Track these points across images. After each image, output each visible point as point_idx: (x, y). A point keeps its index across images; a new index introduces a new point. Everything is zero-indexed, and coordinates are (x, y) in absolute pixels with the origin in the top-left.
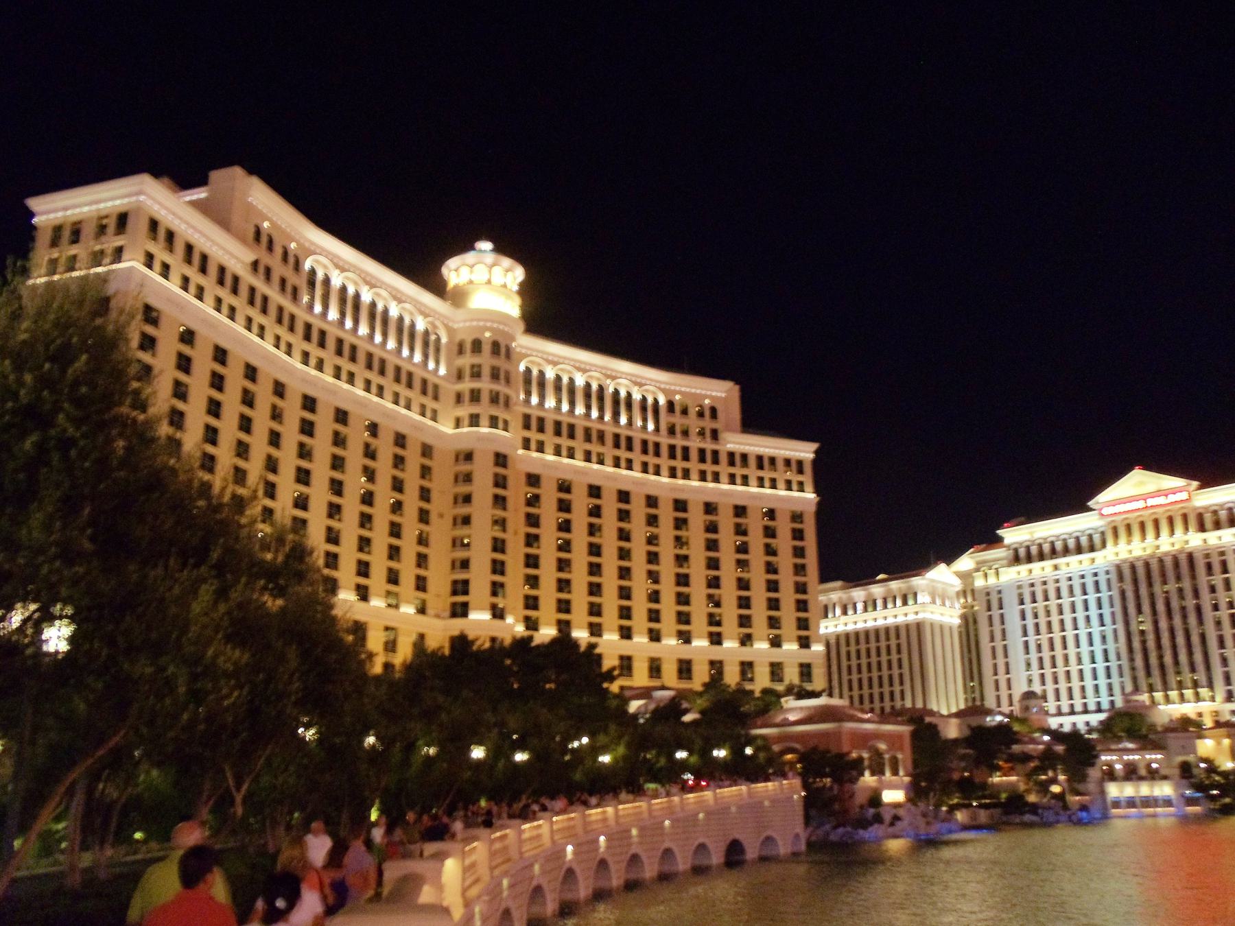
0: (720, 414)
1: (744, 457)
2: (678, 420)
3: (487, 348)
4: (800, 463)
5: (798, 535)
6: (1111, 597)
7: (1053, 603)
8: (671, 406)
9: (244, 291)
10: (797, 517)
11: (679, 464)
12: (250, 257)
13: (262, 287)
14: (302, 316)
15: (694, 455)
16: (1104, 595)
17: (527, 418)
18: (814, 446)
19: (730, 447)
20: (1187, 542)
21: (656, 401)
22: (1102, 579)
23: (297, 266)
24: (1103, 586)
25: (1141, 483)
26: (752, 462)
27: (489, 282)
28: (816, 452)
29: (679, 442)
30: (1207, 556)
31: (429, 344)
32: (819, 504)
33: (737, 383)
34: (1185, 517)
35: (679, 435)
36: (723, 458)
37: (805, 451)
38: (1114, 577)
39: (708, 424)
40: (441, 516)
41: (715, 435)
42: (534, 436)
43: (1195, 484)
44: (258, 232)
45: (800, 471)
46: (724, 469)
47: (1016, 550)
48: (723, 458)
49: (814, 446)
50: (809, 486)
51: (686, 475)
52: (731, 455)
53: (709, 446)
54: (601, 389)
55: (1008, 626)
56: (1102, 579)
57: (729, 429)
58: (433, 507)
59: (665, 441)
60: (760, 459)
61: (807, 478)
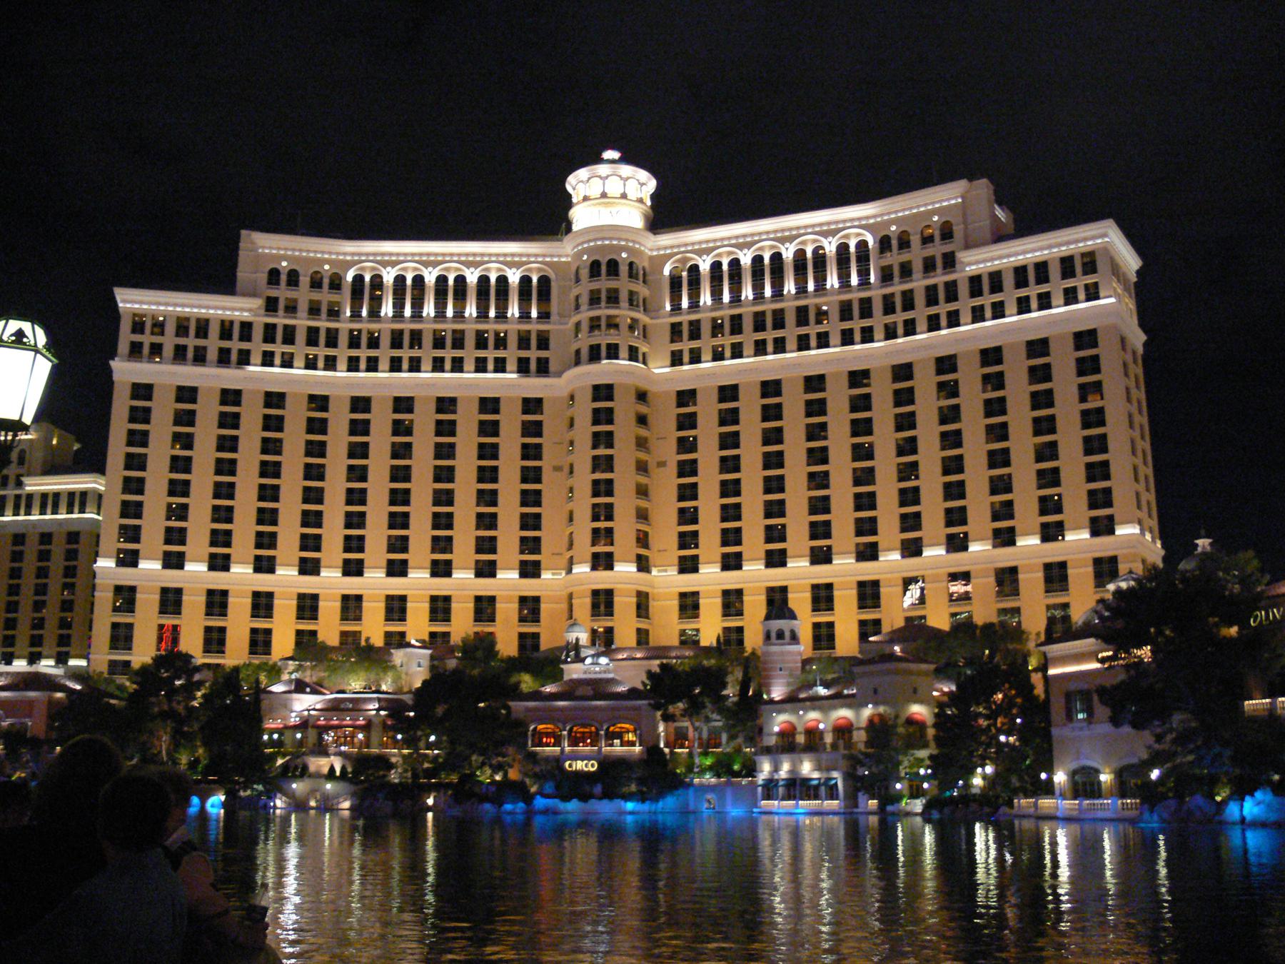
0: (958, 230)
2: (894, 258)
3: (585, 273)
8: (884, 244)
9: (258, 334)
12: (258, 303)
13: (280, 320)
14: (344, 326)
17: (676, 331)
19: (972, 270)
21: (862, 245)
27: (610, 197)
31: (538, 291)
33: (971, 177)
36: (963, 290)
39: (937, 249)
40: (558, 469)
41: (950, 261)
42: (686, 346)
44: (274, 276)
46: (965, 304)
48: (963, 290)
52: (975, 281)
53: (940, 279)
54: (777, 257)
57: (967, 246)
58: (546, 464)
59: (876, 294)
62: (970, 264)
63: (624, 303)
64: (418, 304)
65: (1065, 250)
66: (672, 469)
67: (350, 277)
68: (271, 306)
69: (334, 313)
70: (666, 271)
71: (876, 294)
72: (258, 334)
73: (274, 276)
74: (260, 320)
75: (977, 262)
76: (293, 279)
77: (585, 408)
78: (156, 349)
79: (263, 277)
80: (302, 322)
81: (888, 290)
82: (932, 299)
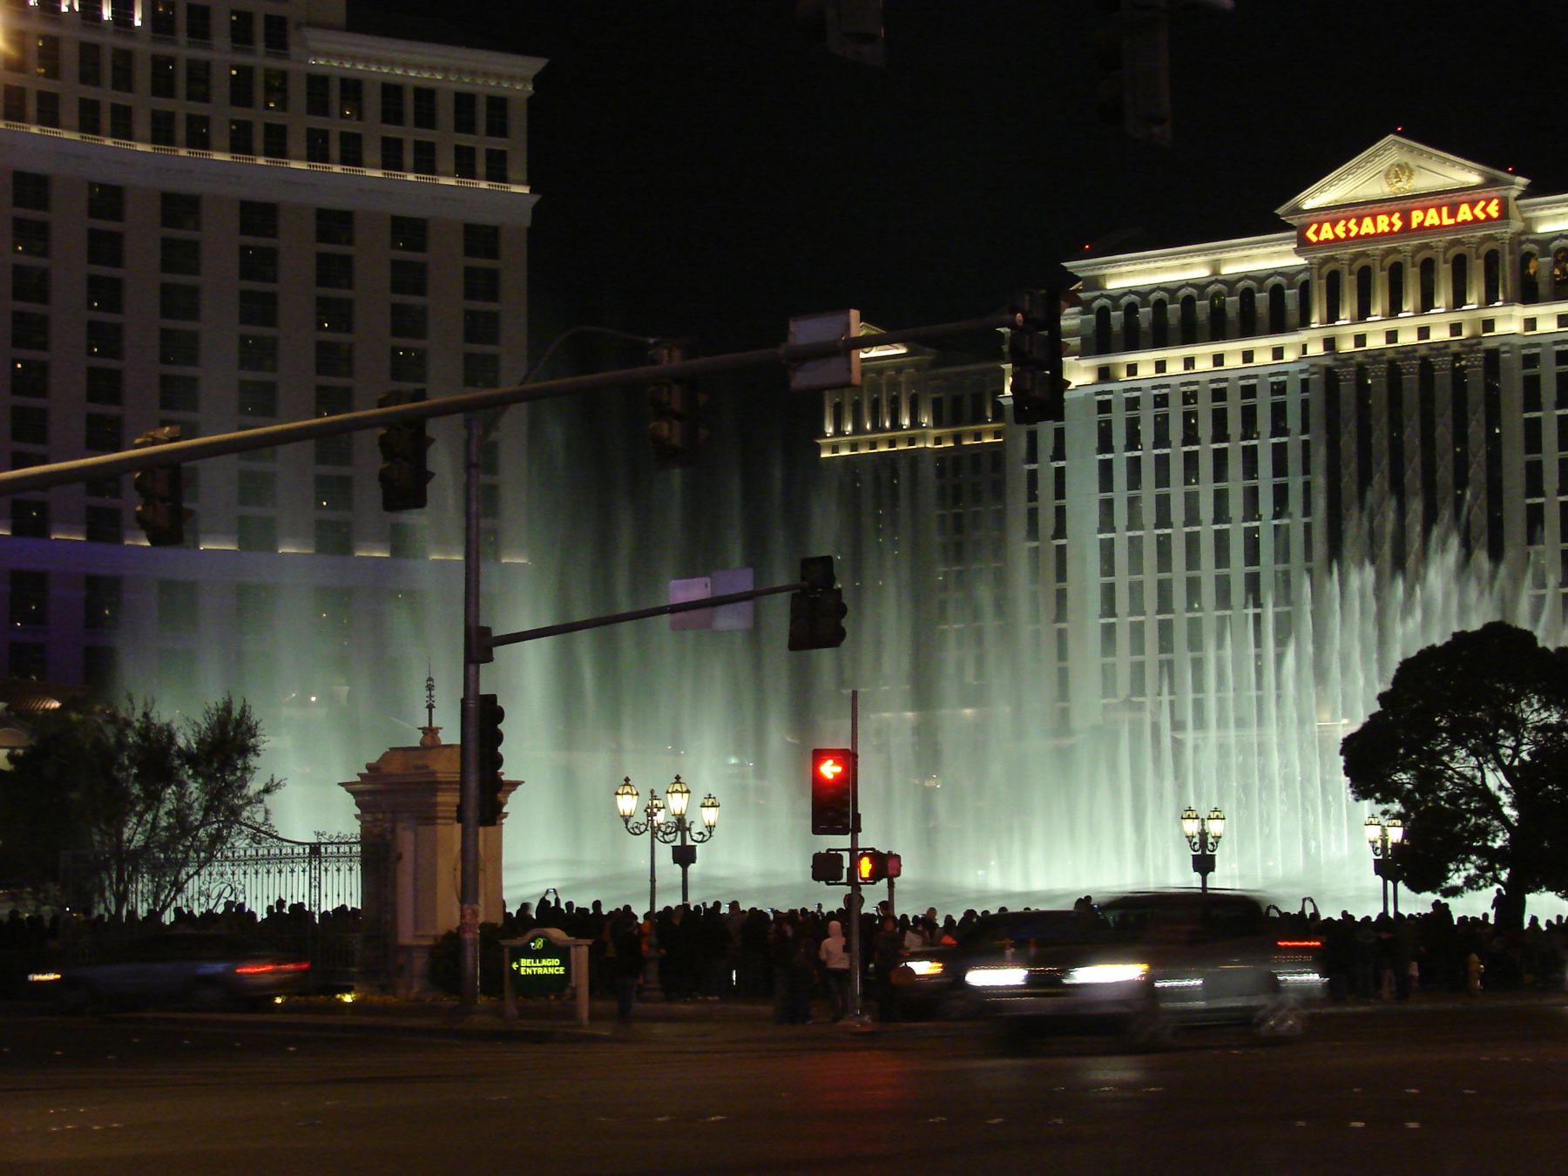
1: (352, 89)
4: (498, 105)
5: (482, 285)
6: (1306, 444)
7: (1147, 453)
10: (481, 239)
11: (181, 107)
15: (221, 89)
16: (1294, 440)
18: (537, 64)
19: (318, 63)
20: (1489, 325)
22: (1293, 399)
24: (1293, 420)
25: (1402, 169)
26: (373, 102)
28: (538, 81)
29: (182, 50)
30: (1531, 361)
32: (536, 209)
34: (1492, 261)
35: (182, 36)
37: (510, 76)
38: (1317, 398)
43: (1521, 181)
45: (498, 127)
47: (1103, 313)
48: (298, 94)
49: (537, 64)
50: (518, 162)
51: (199, 138)
52: (318, 84)
53: (260, 59)
55: (1071, 501)
56: (1293, 399)
59: (144, 50)
60: (392, 92)
61: (516, 145)
62: (316, 54)
65: (466, 84)
71: (144, 50)
75: (328, 55)
81: (166, 50)
82: (241, 91)
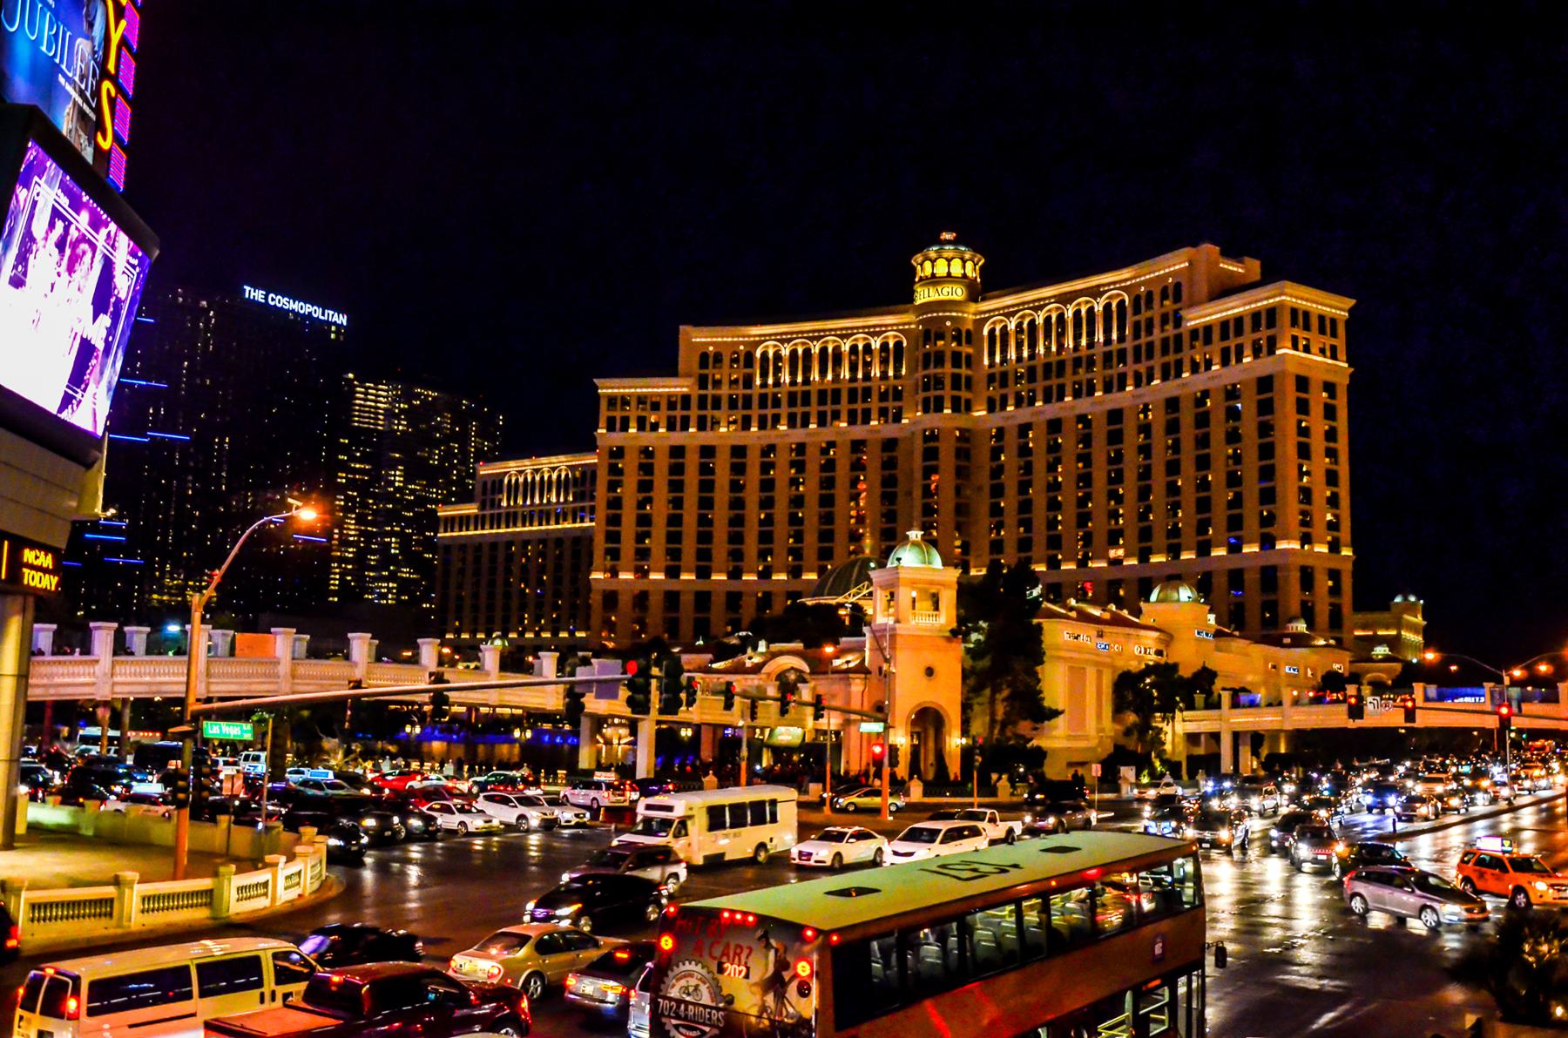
9: (694, 402)
13: (710, 391)
23: (749, 357)
63: (948, 365)
64: (807, 370)
66: (987, 490)
67: (758, 354)
68: (703, 382)
69: (748, 382)
70: (985, 332)
72: (694, 402)
73: (704, 358)
74: (696, 393)
76: (718, 358)
77: (919, 445)
78: (672, 406)
79: (697, 359)
80: (725, 391)
